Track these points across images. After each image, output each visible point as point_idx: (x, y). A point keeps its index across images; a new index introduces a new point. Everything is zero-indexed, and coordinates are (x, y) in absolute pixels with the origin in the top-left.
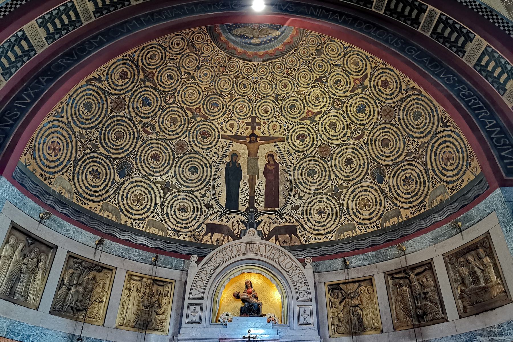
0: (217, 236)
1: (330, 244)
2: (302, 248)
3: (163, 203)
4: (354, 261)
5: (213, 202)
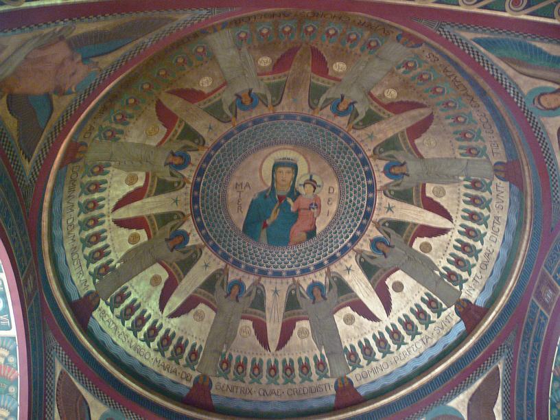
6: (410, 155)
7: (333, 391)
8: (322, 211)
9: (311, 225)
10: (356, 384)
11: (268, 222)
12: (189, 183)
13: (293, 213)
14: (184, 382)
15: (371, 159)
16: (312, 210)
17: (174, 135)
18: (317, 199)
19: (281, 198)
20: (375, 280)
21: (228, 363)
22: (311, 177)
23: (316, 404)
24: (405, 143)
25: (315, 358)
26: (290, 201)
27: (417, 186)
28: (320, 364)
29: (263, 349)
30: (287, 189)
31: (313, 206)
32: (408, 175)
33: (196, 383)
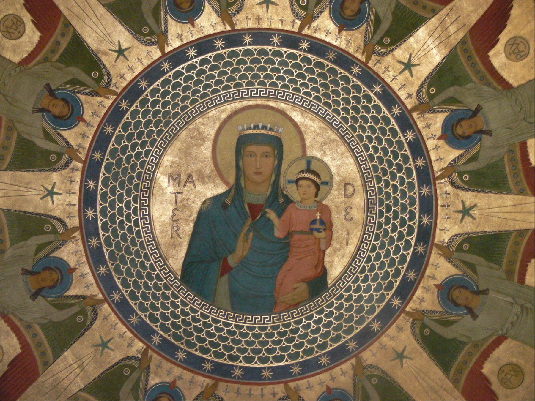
6: (486, 88)
8: (335, 236)
9: (316, 267)
11: (232, 261)
12: (79, 160)
13: (279, 239)
15: (415, 115)
16: (316, 234)
17: (53, 51)
18: (326, 210)
19: (255, 209)
20: (459, 371)
22: (309, 163)
24: (473, 65)
26: (272, 215)
27: (511, 151)
30: (266, 190)
31: (318, 226)
32: (489, 133)
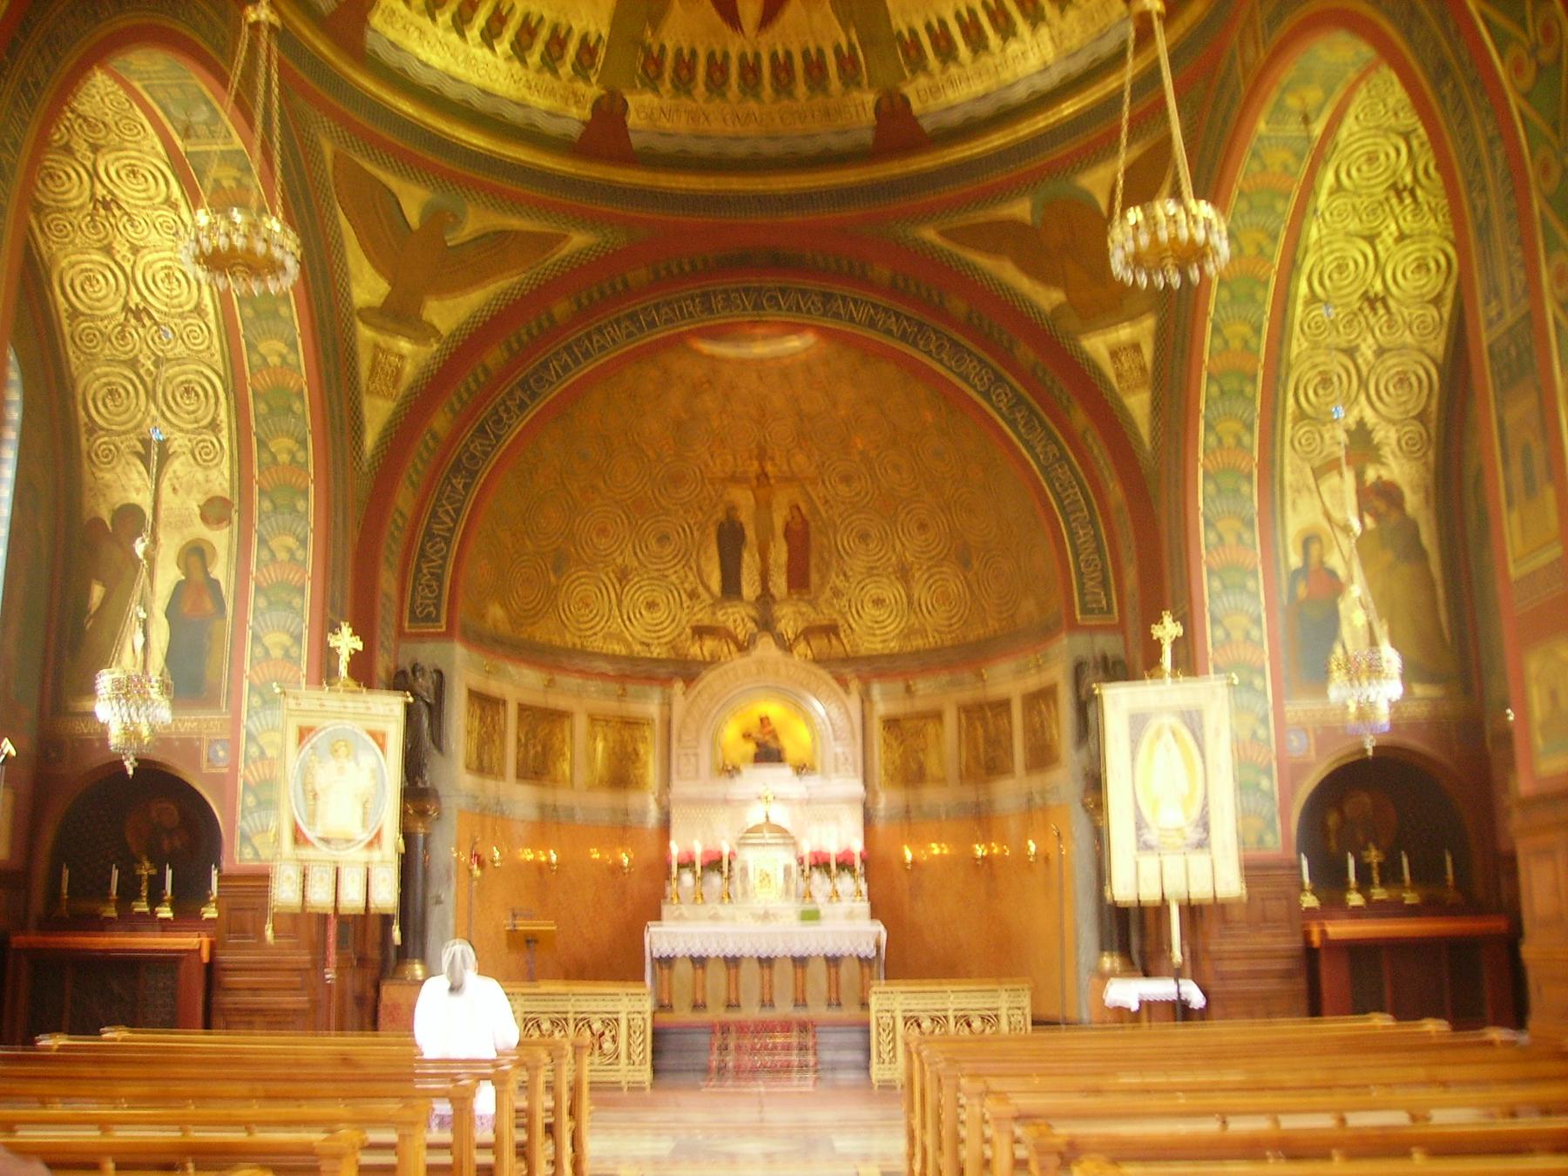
0: (710, 644)
1: (891, 657)
2: (847, 660)
3: (620, 602)
4: (922, 686)
5: (701, 589)
7: (869, 116)
10: (916, 106)
14: (574, 112)
21: (659, 63)
23: (836, 143)
25: (837, 50)
28: (848, 64)
29: (727, 30)
33: (597, 106)
